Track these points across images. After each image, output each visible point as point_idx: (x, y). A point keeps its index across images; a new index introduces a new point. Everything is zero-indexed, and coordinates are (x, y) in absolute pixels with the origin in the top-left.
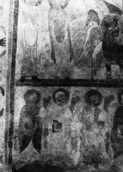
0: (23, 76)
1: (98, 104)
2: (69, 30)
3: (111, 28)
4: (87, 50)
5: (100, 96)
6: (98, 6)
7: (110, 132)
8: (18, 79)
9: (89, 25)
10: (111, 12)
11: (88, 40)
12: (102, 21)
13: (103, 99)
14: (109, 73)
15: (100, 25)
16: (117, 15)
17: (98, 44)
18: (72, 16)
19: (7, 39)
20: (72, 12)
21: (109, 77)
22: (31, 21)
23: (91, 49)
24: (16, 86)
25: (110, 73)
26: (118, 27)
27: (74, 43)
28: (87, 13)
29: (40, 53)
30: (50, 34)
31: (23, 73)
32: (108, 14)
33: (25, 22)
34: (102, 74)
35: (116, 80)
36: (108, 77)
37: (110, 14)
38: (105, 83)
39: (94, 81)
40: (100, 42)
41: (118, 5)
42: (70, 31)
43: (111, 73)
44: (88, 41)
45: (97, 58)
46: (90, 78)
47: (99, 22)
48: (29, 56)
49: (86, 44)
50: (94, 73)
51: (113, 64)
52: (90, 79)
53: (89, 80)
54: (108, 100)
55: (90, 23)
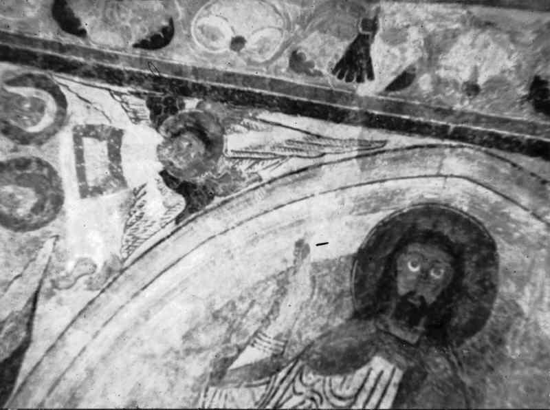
41: (20, 390)
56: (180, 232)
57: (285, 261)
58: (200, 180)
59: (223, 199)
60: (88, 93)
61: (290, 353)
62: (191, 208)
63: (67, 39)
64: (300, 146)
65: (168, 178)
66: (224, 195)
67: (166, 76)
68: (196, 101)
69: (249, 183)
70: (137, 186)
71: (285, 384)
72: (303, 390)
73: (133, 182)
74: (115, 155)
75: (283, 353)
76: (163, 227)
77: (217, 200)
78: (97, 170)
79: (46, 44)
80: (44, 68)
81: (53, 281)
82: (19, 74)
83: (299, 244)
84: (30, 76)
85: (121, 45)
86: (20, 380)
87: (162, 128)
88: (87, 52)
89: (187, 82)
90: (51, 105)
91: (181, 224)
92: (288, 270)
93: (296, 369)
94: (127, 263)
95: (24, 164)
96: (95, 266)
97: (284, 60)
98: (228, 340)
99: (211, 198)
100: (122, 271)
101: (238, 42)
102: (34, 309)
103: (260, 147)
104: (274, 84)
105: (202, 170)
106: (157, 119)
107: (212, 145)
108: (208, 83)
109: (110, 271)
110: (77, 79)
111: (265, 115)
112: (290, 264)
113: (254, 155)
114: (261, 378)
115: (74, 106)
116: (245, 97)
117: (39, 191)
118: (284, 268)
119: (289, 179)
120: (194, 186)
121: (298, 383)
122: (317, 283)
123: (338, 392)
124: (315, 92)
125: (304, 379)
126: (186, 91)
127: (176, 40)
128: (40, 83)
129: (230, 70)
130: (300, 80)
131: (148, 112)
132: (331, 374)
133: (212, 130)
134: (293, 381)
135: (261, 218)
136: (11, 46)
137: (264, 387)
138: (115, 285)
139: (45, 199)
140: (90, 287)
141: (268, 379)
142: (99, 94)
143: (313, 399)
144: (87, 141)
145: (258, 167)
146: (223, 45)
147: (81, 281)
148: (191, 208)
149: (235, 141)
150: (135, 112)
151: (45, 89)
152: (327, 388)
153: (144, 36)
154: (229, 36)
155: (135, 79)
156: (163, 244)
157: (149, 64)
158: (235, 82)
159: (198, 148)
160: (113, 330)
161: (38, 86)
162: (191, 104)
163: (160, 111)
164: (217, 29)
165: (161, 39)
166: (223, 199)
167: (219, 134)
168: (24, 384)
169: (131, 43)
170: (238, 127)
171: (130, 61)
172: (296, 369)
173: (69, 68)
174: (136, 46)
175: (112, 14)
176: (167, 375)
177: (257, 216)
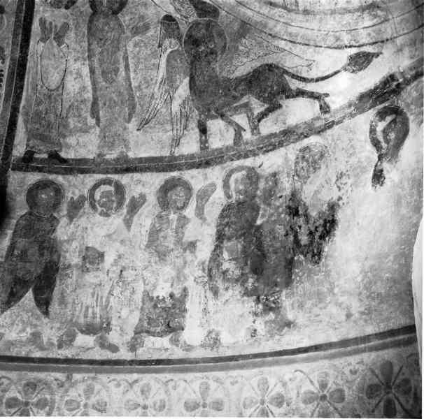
0: (28, 151)
1: (183, 208)
2: (127, 57)
3: (203, 48)
4: (161, 98)
5: (189, 189)
7: (208, 259)
8: (18, 155)
10: (200, 15)
12: (187, 35)
13: (194, 198)
15: (183, 46)
17: (181, 82)
18: (133, 28)
19: (6, 73)
20: (131, 22)
22: (54, 38)
23: (169, 93)
24: (13, 169)
25: (206, 137)
26: (215, 43)
27: (137, 84)
28: (158, 22)
29: (70, 103)
30: (89, 65)
31: (31, 143)
32: (195, 19)
33: (43, 39)
34: (190, 146)
35: (217, 149)
37: (199, 19)
38: (197, 160)
40: (185, 77)
42: (130, 61)
44: (162, 78)
46: (168, 154)
47: (182, 37)
48: (47, 109)
49: (161, 83)
50: (176, 142)
51: (213, 117)
52: (169, 156)
53: (166, 157)
54: (204, 195)
55: (167, 42)
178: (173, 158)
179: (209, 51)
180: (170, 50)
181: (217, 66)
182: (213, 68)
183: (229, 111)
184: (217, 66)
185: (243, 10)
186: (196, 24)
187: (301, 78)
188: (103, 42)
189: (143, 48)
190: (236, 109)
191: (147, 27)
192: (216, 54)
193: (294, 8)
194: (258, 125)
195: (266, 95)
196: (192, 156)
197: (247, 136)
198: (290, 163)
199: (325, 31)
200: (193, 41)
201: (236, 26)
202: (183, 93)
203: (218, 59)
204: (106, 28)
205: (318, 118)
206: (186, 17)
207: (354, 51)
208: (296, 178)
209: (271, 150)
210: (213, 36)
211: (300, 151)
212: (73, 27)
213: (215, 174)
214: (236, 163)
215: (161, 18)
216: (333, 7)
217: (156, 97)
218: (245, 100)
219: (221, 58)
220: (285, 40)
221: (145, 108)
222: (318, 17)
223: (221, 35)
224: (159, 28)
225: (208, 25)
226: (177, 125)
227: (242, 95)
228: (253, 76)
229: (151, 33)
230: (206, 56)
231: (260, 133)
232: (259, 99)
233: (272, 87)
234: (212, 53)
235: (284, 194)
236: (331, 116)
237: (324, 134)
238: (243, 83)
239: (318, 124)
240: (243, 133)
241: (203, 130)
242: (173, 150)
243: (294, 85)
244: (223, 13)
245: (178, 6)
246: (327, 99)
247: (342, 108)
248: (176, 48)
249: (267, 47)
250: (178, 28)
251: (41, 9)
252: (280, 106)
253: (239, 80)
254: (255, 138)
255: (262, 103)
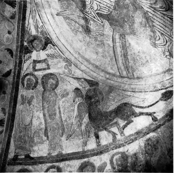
0: (16, 155)
2: (60, 108)
3: (93, 100)
6: (81, 84)
8: (11, 157)
9: (76, 102)
11: (77, 114)
12: (86, 95)
14: (98, 140)
15: (84, 100)
16: (96, 87)
17: (85, 116)
18: (61, 95)
19: (6, 120)
20: (61, 92)
21: (99, 144)
22: (27, 103)
23: (80, 122)
24: (8, 165)
27: (65, 119)
28: (73, 91)
29: (35, 131)
30: (43, 113)
31: (17, 151)
32: (89, 88)
33: (23, 103)
34: (92, 145)
35: (105, 145)
36: (97, 144)
37: (90, 88)
38: (96, 151)
39: (85, 152)
40: (86, 114)
42: (61, 109)
43: (100, 140)
45: (86, 129)
46: (82, 150)
48: (24, 134)
50: (85, 144)
51: (101, 130)
52: (82, 151)
53: (81, 152)
55: (77, 99)
56: (57, 45)
57: (61, 18)
58: (44, 40)
59: (48, 35)
60: (25, 68)
61: (82, 15)
62: (51, 43)
63: (12, 74)
64: (33, 16)
65: (44, 48)
66: (47, 34)
67: (19, 50)
68: (24, 42)
69: (43, 28)
70: (46, 56)
71: (89, 16)
72: (90, 11)
73: (46, 57)
74: (39, 62)
75: (82, 17)
76: (56, 49)
77: (48, 36)
78: (44, 65)
79: (14, 78)
80: (20, 79)
81: (70, 74)
82: (21, 84)
83: (57, 15)
84: (22, 82)
85: (12, 61)
86: (92, 79)
87: (32, 50)
88: (15, 69)
89: (20, 45)
90: (28, 77)
91: (55, 45)
92: (63, 17)
93: (86, 13)
94: (64, 57)
95: (43, 83)
96: (66, 65)
97: (12, 21)
98: (81, 31)
99: (48, 38)
100: (67, 58)
101: (9, 33)
102: (76, 78)
103: (34, 26)
104: (19, 23)
105: (41, 40)
106: (31, 52)
107: (35, 38)
108: (20, 40)
109: (67, 61)
110: (22, 71)
111: (26, 25)
112: (62, 17)
113: (37, 27)
114: (88, 22)
115: (28, 71)
116: (23, 30)
117: (49, 79)
118: (63, 18)
119: (41, 18)
120: (45, 42)
121: (89, 13)
122: (65, 10)
123: (90, 2)
124: (20, 13)
125: (87, 11)
126: (22, 45)
127: (10, 48)
128: (23, 79)
129: (16, 34)
130: (17, 16)
131: (28, 54)
132: (86, 5)
133: (31, 38)
134: (88, 14)
135: (52, 25)
136: (15, 86)
137: (91, 21)
138: (70, 60)
139: (51, 77)
140: (71, 66)
141: (88, 20)
142: (25, 66)
143: (92, 9)
144: (36, 68)
145: (39, 26)
146: (10, 36)
147: (69, 68)
148: (51, 43)
149: (34, 32)
150: (29, 57)
151: (25, 78)
152: (89, 5)
153: (10, 56)
154: (8, 35)
155: (20, 57)
156: (60, 49)
157: (16, 54)
158: (19, 33)
159: (36, 41)
160: (80, 59)
161: (24, 80)
162: (25, 44)
163: (28, 51)
164: (6, 38)
165: (10, 51)
166: (48, 35)
167: (32, 37)
168: (93, 78)
169: (12, 59)
170: (30, 31)
171: (16, 58)
172: (86, 13)
173: (19, 73)
174: (12, 58)
175: (5, 64)
176: (90, 45)
177: (51, 26)
178: (84, 152)
179: (96, 101)
180: (79, 102)
181: (100, 107)
182: (99, 108)
183: (108, 126)
184: (100, 107)
185: (109, 81)
186: (89, 90)
187: (140, 107)
188: (49, 102)
189: (67, 103)
190: (111, 125)
191: (68, 94)
192: (99, 101)
193: (132, 77)
194: (123, 131)
195: (125, 117)
196: (93, 150)
197: (119, 137)
198: (142, 147)
199: (148, 84)
200: (88, 98)
201: (107, 88)
202: (86, 121)
203: (101, 104)
204: (50, 96)
205: (152, 124)
206: (85, 88)
207: (164, 91)
208: (147, 155)
209: (131, 143)
210: (97, 94)
211: (146, 141)
212: (36, 97)
213: (105, 158)
214: (115, 151)
215: (74, 89)
216: (150, 74)
217: (74, 124)
218: (115, 120)
219: (102, 104)
220: (130, 91)
221: (69, 129)
222: (144, 79)
223: (101, 93)
224: (73, 94)
225: (95, 89)
226: (84, 136)
227: (114, 119)
228: (118, 109)
229: (69, 96)
230: (95, 103)
231: (124, 135)
232: (122, 120)
233: (127, 113)
234: (97, 102)
235: (142, 164)
236: (158, 122)
237: (157, 131)
238: (113, 113)
239: (153, 127)
240: (117, 136)
241: (97, 137)
242: (84, 148)
243: (138, 110)
244: (101, 84)
245: (81, 84)
246: (155, 115)
247: (163, 118)
248: (81, 101)
249: (122, 96)
250: (81, 93)
251: (22, 91)
252: (132, 121)
253: (111, 112)
254: (123, 137)
255: (124, 121)
